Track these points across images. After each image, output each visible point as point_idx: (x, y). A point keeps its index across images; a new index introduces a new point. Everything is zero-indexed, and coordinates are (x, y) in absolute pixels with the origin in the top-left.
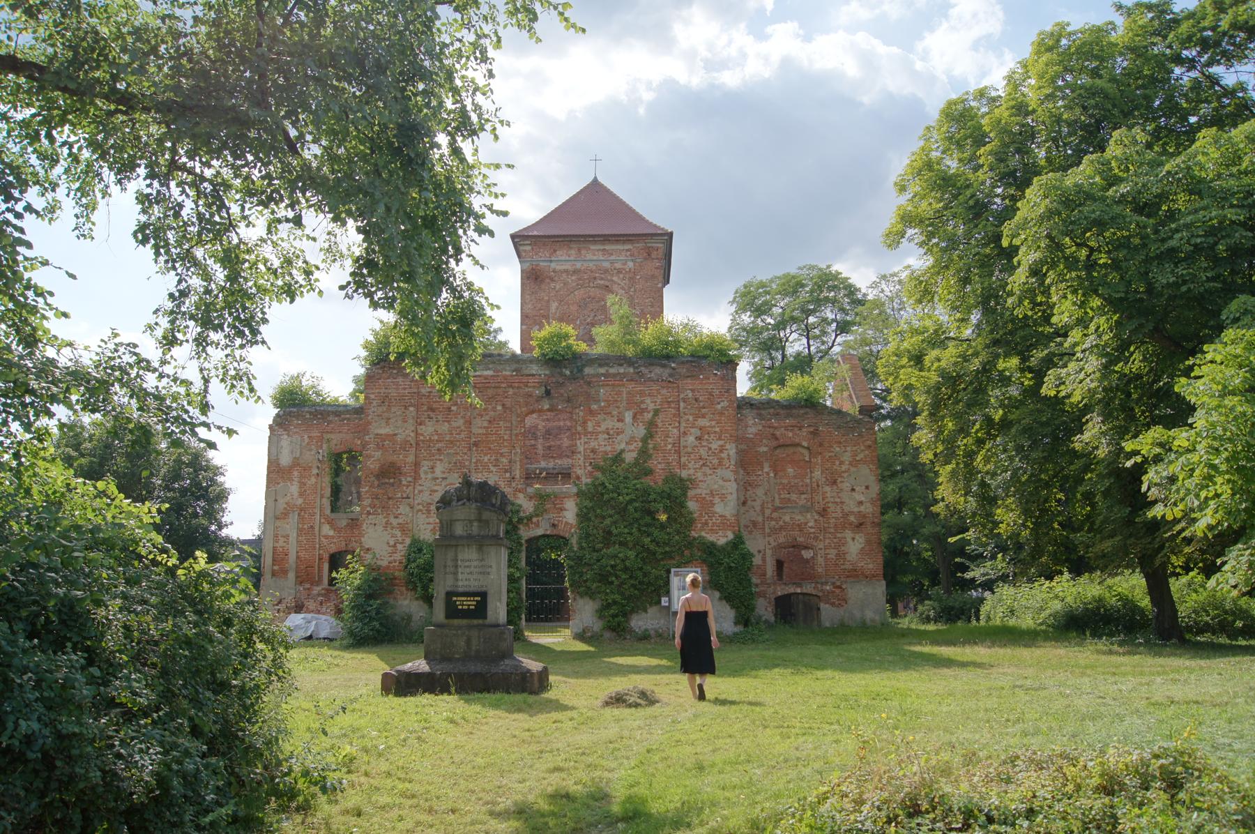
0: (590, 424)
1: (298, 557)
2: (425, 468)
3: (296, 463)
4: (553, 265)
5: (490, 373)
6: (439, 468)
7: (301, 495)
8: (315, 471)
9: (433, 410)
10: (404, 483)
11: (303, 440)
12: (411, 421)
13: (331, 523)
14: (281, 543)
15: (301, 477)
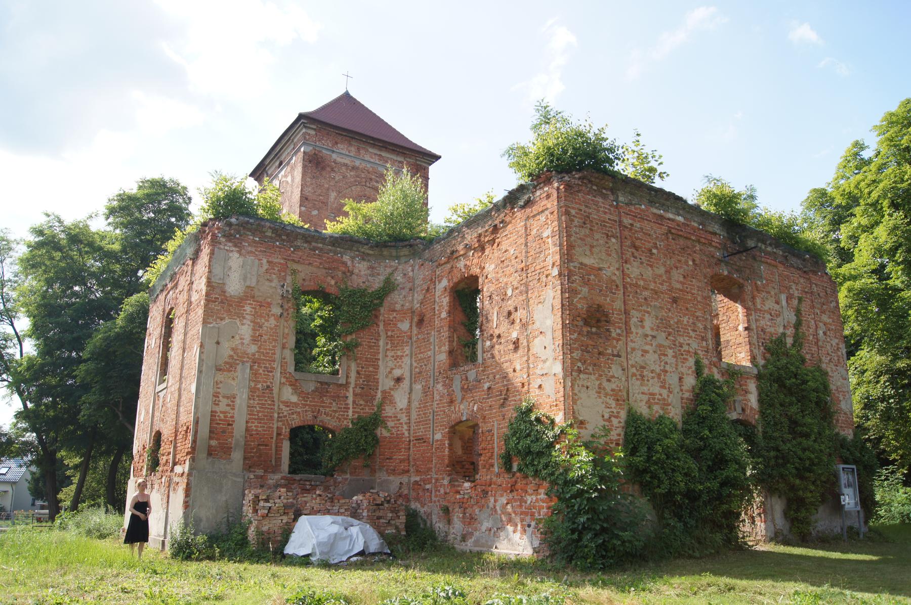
0: (758, 301)
1: (247, 430)
2: (635, 320)
3: (249, 295)
4: (334, 156)
5: (680, 219)
6: (648, 323)
7: (255, 339)
8: (277, 310)
9: (636, 248)
10: (614, 335)
11: (261, 265)
12: (614, 255)
13: (294, 384)
14: (223, 406)
15: (256, 315)
